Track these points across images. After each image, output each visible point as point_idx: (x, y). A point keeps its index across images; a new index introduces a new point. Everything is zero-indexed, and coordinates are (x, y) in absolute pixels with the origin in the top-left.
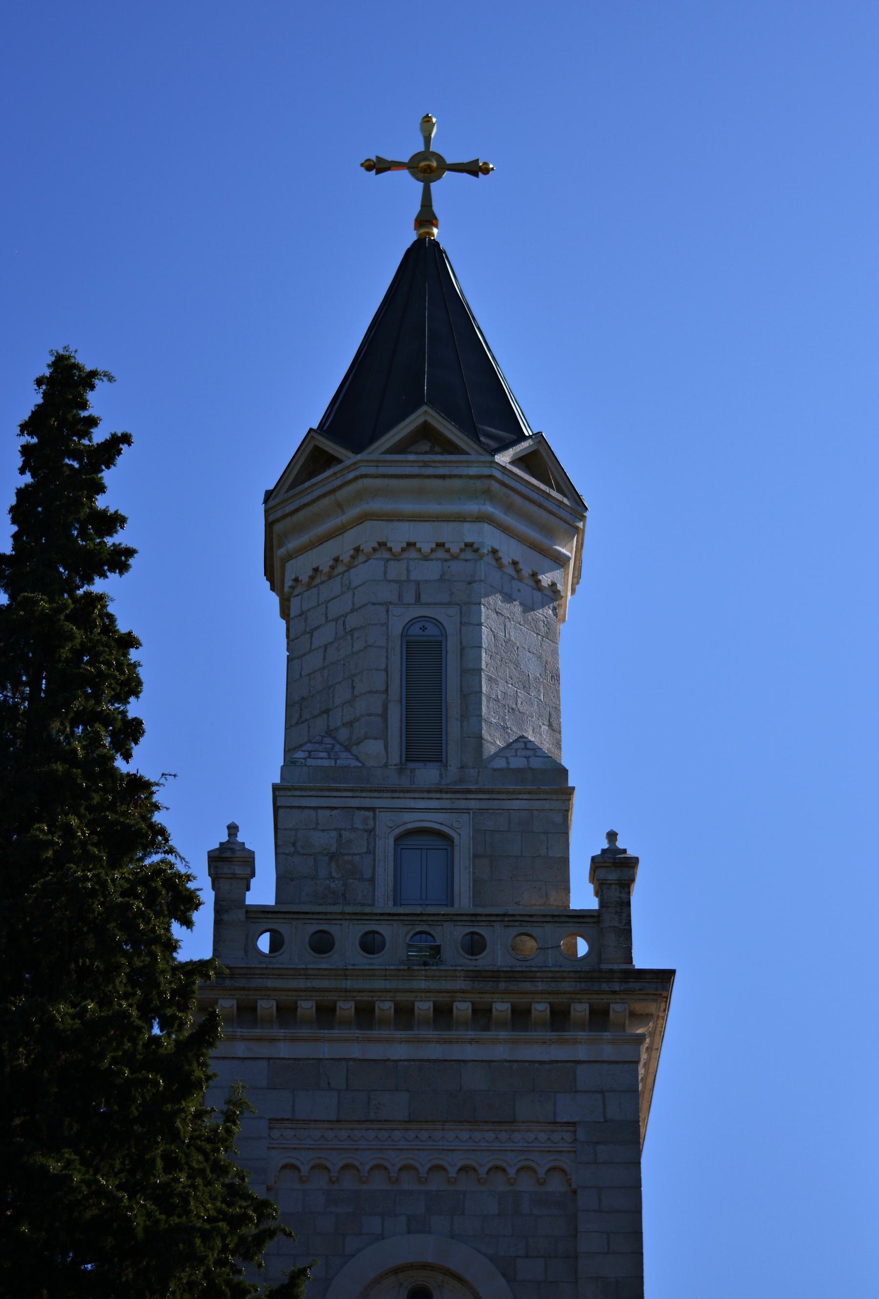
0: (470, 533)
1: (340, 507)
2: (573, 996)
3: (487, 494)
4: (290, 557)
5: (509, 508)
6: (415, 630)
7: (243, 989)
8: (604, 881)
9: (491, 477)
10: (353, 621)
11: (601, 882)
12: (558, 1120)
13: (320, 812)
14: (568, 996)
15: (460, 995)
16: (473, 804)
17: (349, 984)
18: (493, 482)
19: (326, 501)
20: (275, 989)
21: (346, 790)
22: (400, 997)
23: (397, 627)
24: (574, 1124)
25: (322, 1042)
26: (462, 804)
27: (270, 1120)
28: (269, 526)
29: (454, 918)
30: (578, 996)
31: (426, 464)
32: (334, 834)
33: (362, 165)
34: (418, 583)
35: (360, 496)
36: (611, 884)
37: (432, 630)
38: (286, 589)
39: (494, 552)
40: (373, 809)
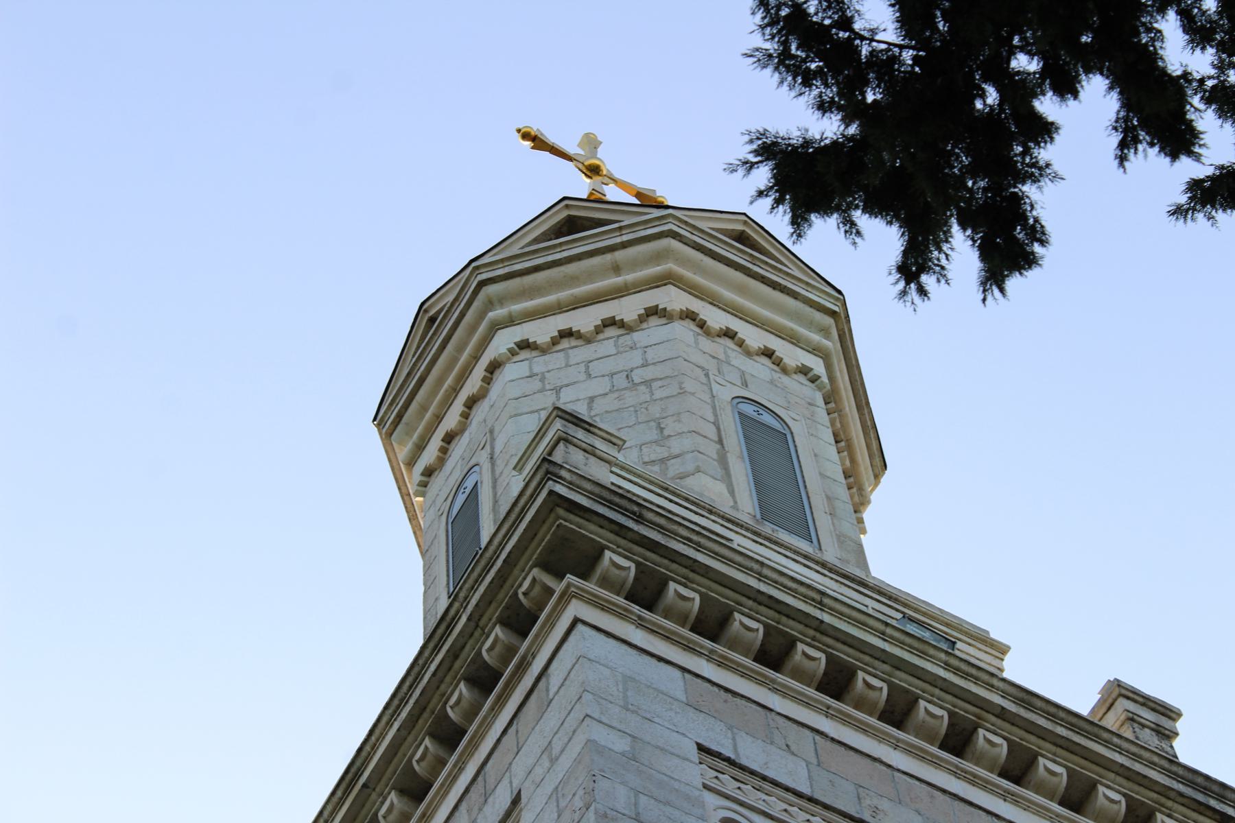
2: (1163, 800)
3: (825, 332)
7: (653, 546)
8: (1135, 717)
11: (1131, 715)
14: (1155, 796)
15: (993, 719)
19: (596, 260)
20: (706, 571)
22: (903, 680)
25: (770, 689)
27: (701, 748)
30: (1170, 803)
33: (519, 131)
35: (658, 257)
36: (1144, 726)
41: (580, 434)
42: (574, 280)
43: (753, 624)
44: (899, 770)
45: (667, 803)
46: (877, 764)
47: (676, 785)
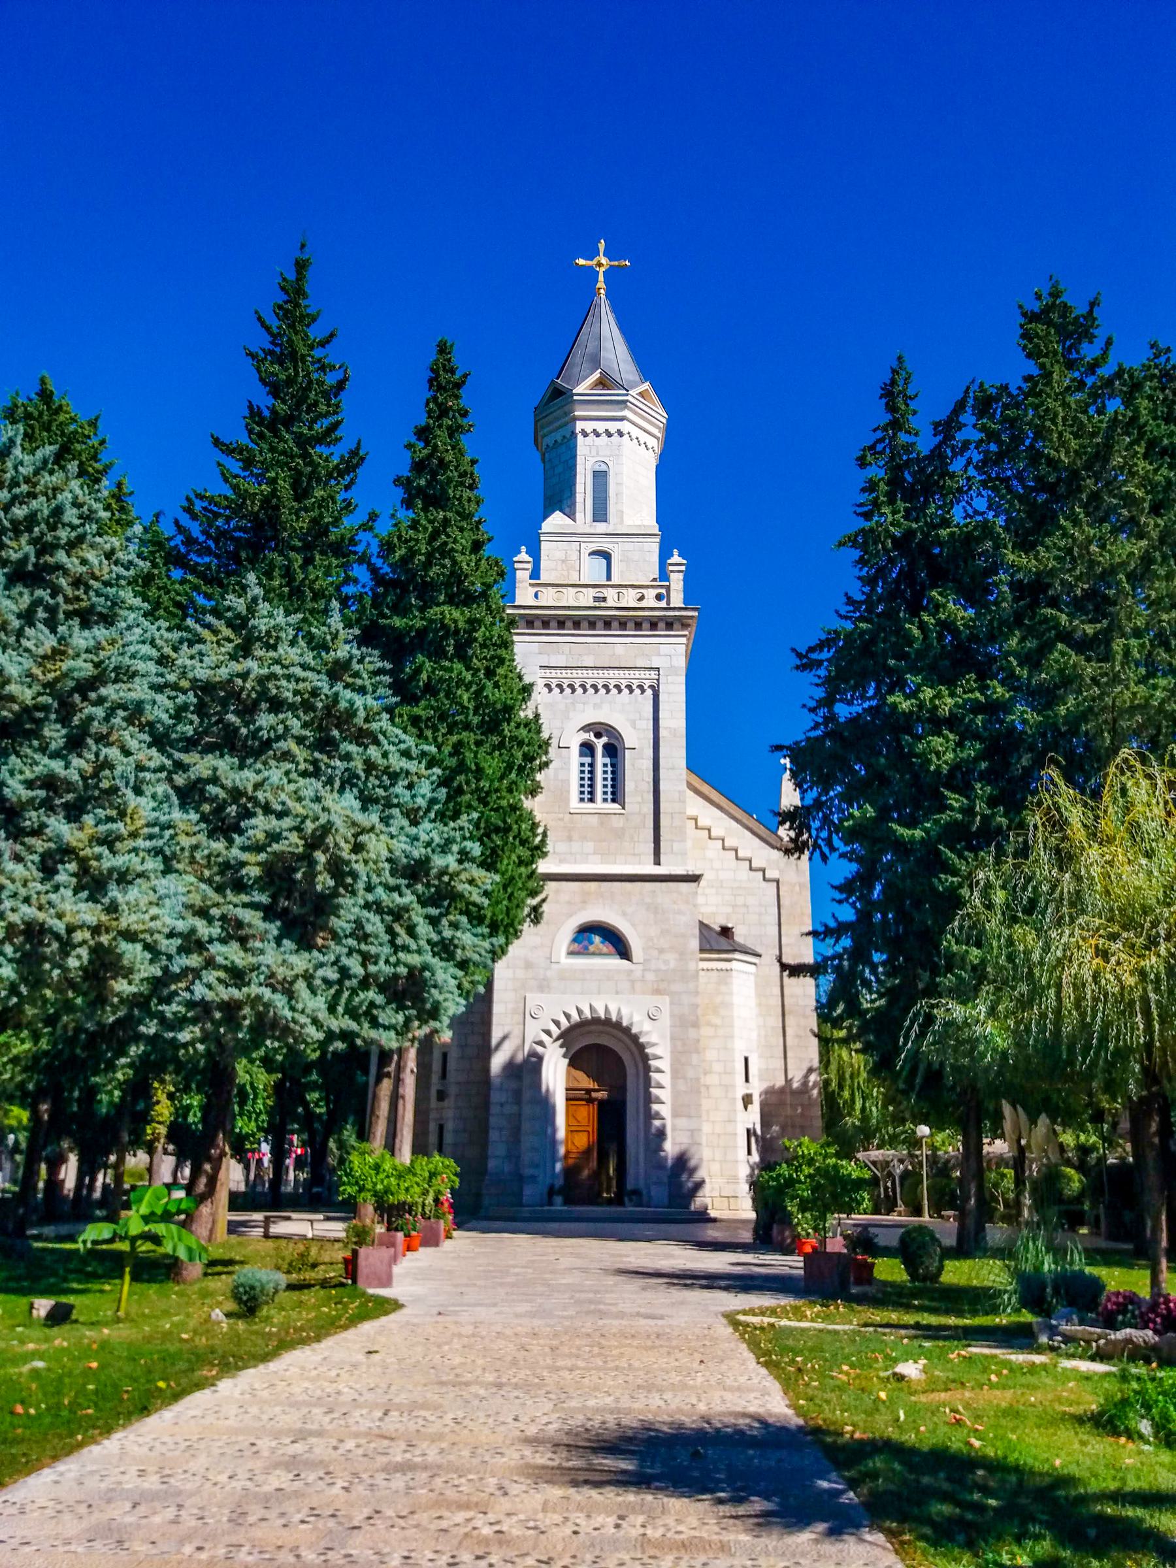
29: (612, 586)
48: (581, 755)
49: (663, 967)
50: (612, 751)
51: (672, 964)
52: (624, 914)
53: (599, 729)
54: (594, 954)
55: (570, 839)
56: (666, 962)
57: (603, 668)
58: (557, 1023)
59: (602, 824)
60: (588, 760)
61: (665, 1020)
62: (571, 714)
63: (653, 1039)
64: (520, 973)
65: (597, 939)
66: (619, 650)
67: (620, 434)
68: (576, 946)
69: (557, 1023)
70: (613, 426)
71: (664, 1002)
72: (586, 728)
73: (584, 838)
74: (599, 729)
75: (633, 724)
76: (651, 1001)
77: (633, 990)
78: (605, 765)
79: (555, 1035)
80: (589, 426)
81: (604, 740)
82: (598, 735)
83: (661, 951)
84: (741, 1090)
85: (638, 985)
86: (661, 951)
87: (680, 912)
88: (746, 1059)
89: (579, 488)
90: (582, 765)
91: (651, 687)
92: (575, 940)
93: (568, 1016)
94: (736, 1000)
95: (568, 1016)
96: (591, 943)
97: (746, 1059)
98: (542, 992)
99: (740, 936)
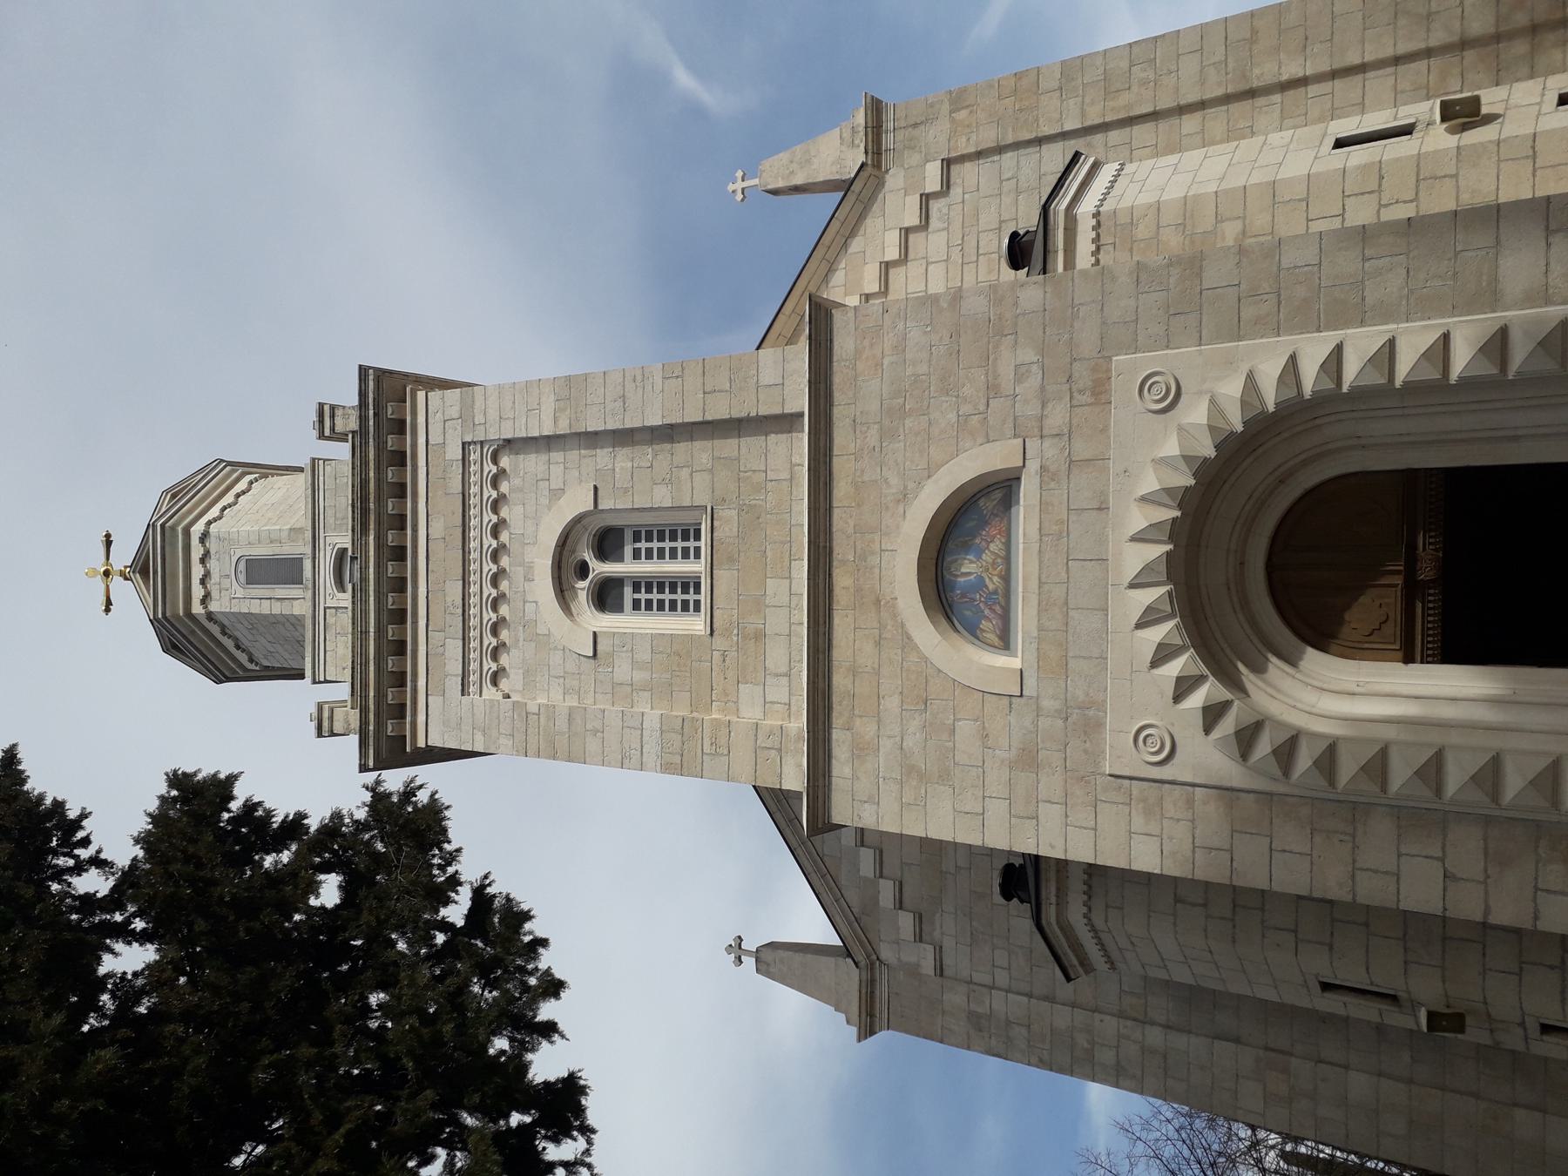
0: (195, 541)
1: (193, 632)
3: (173, 528)
4: (241, 666)
5: (190, 512)
6: (242, 577)
9: (163, 526)
10: (246, 623)
12: (461, 457)
13: (327, 649)
16: (322, 535)
17: (372, 630)
18: (168, 525)
21: (314, 630)
23: (240, 593)
24: (464, 444)
26: (322, 541)
27: (463, 695)
28: (229, 680)
31: (155, 572)
32: (338, 636)
34: (221, 576)
37: (242, 566)
38: (258, 668)
39: (209, 523)
40: (325, 608)
41: (326, 724)
42: (208, 647)
43: (390, 662)
44: (427, 588)
45: (498, 717)
46: (430, 598)
47: (488, 712)
48: (618, 608)
49: (1034, 381)
50: (608, 543)
51: (1028, 355)
52: (904, 497)
53: (566, 570)
54: (1007, 578)
55: (760, 636)
56: (1020, 373)
57: (465, 562)
58: (1183, 688)
59: (731, 560)
60: (628, 591)
61: (1180, 360)
62: (541, 630)
63: (1232, 389)
64: (1051, 783)
65: (968, 568)
66: (437, 529)
67: (204, 537)
68: (988, 627)
69: (1183, 688)
70: (197, 551)
71: (1128, 366)
72: (563, 592)
73: (759, 604)
74: (568, 571)
75: (557, 494)
76: (1127, 409)
77: (1097, 461)
78: (636, 555)
79: (1223, 694)
80: (197, 592)
81: (588, 556)
82: (583, 570)
83: (992, 390)
84: (1439, 139)
85: (1081, 449)
86: (992, 390)
87: (900, 348)
88: (1340, 144)
89: (265, 608)
90: (636, 605)
91: (495, 461)
92: (972, 631)
93: (1163, 655)
94: (1174, 193)
95: (1163, 655)
96: (980, 584)
97: (1340, 144)
98: (1100, 725)
99: (1028, 220)
